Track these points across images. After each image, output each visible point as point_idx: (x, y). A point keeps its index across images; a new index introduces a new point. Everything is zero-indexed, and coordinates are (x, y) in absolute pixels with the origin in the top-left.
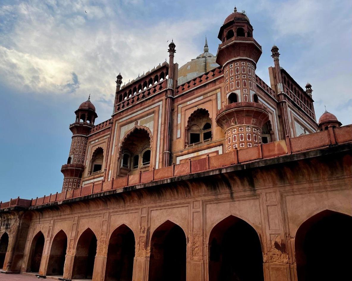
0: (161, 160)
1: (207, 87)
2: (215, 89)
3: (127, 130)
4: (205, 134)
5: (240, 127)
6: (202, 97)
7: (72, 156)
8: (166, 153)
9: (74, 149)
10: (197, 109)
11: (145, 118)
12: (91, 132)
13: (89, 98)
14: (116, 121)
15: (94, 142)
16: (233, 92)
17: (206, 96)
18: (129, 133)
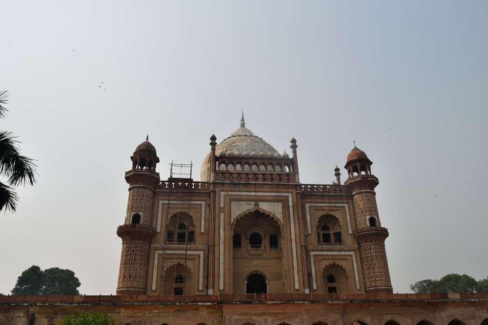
4: (323, 234)
7: (141, 214)
16: (373, 216)
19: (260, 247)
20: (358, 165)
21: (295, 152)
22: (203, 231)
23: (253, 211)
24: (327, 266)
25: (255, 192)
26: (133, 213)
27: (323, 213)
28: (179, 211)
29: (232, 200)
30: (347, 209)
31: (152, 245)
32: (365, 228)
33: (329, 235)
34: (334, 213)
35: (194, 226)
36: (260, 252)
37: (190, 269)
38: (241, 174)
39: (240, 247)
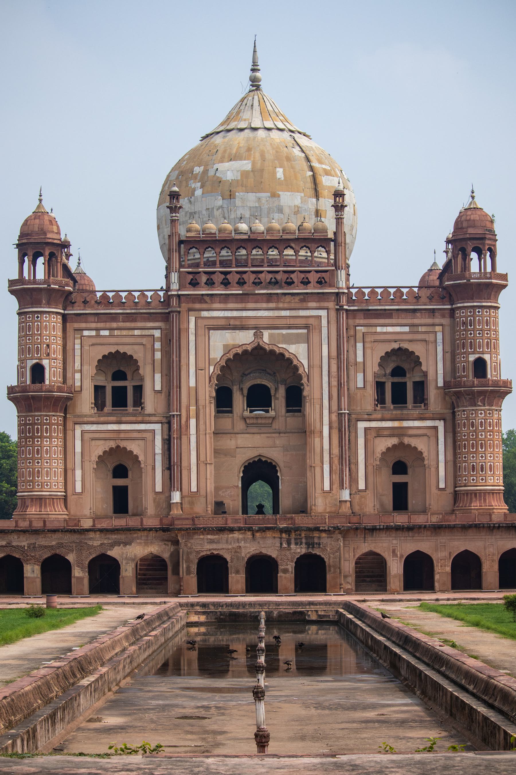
0: (335, 425)
1: (418, 314)
2: (434, 325)
3: (231, 342)
4: (393, 384)
5: (489, 410)
6: (407, 329)
7: (45, 363)
8: (345, 413)
9: (48, 346)
10: (399, 347)
11: (284, 332)
13: (40, 200)
14: (190, 310)
15: (93, 333)
17: (415, 329)
18: (240, 351)
19: (267, 411)
21: (339, 221)
22: (158, 387)
23: (249, 348)
24: (388, 449)
26: (30, 363)
27: (389, 347)
28: (113, 349)
29: (210, 329)
30: (440, 336)
32: (465, 376)
33: (405, 383)
34: (411, 347)
35: (142, 379)
36: (267, 421)
37: (137, 457)
39: (231, 412)
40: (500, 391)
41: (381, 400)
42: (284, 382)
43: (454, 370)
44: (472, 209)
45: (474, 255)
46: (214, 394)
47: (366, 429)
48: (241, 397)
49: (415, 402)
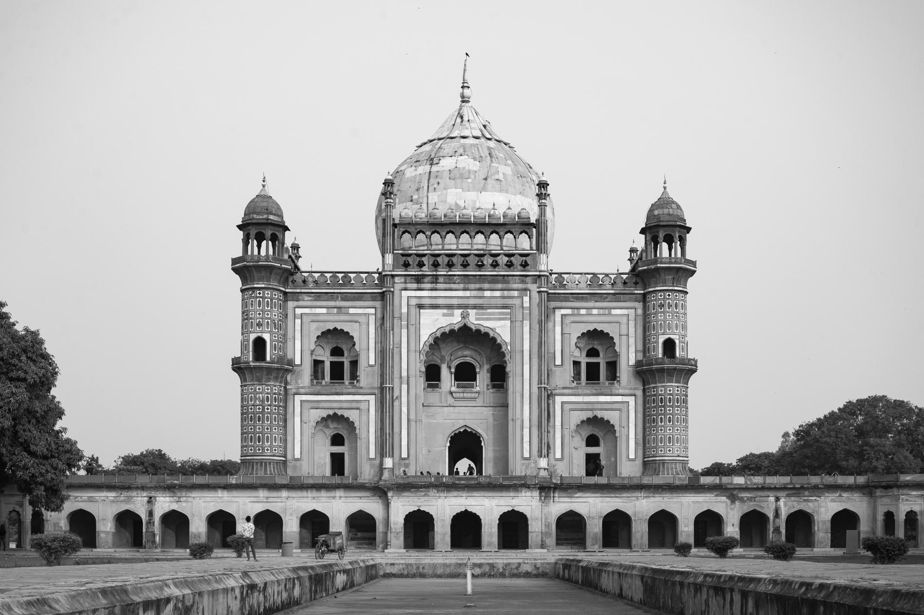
4: (588, 364)
7: (266, 337)
12: (294, 282)
16: (672, 337)
20: (661, 235)
21: (542, 212)
22: (372, 362)
24: (583, 422)
25: (465, 289)
26: (253, 337)
28: (331, 327)
29: (421, 307)
31: (288, 387)
33: (599, 363)
34: (606, 328)
36: (473, 395)
38: (439, 255)
40: (687, 370)
41: (577, 376)
42: (489, 360)
43: (645, 350)
44: (664, 202)
45: (665, 246)
46: (424, 369)
47: (563, 403)
48: (449, 375)
49: (607, 379)
